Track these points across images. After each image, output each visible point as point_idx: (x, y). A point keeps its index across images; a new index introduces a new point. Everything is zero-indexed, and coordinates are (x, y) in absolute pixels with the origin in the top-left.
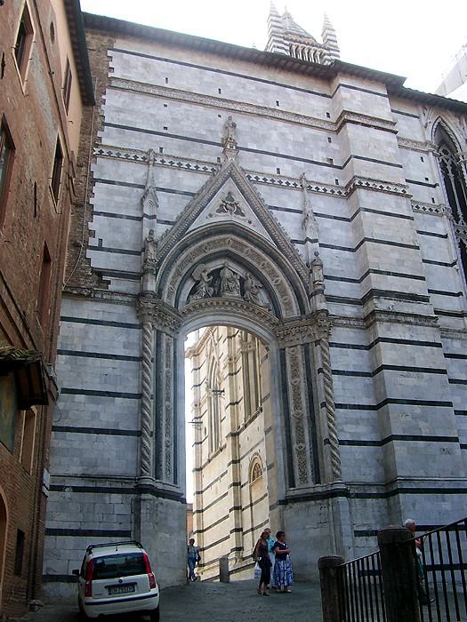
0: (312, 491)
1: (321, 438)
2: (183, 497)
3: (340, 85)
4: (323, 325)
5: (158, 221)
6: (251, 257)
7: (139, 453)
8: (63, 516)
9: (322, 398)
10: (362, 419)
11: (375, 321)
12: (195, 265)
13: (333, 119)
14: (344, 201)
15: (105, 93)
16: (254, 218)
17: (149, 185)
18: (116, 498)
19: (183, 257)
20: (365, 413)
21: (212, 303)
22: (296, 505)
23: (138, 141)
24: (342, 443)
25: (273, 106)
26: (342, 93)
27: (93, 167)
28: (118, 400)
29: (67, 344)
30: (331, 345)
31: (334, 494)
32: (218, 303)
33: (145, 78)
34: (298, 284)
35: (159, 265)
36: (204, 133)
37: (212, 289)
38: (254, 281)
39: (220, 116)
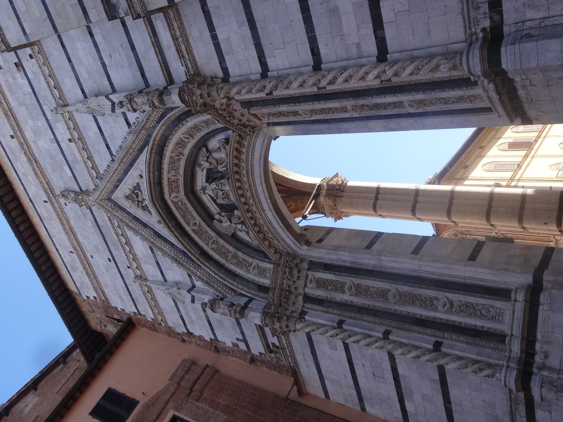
6: (177, 170)
28: (401, 370)
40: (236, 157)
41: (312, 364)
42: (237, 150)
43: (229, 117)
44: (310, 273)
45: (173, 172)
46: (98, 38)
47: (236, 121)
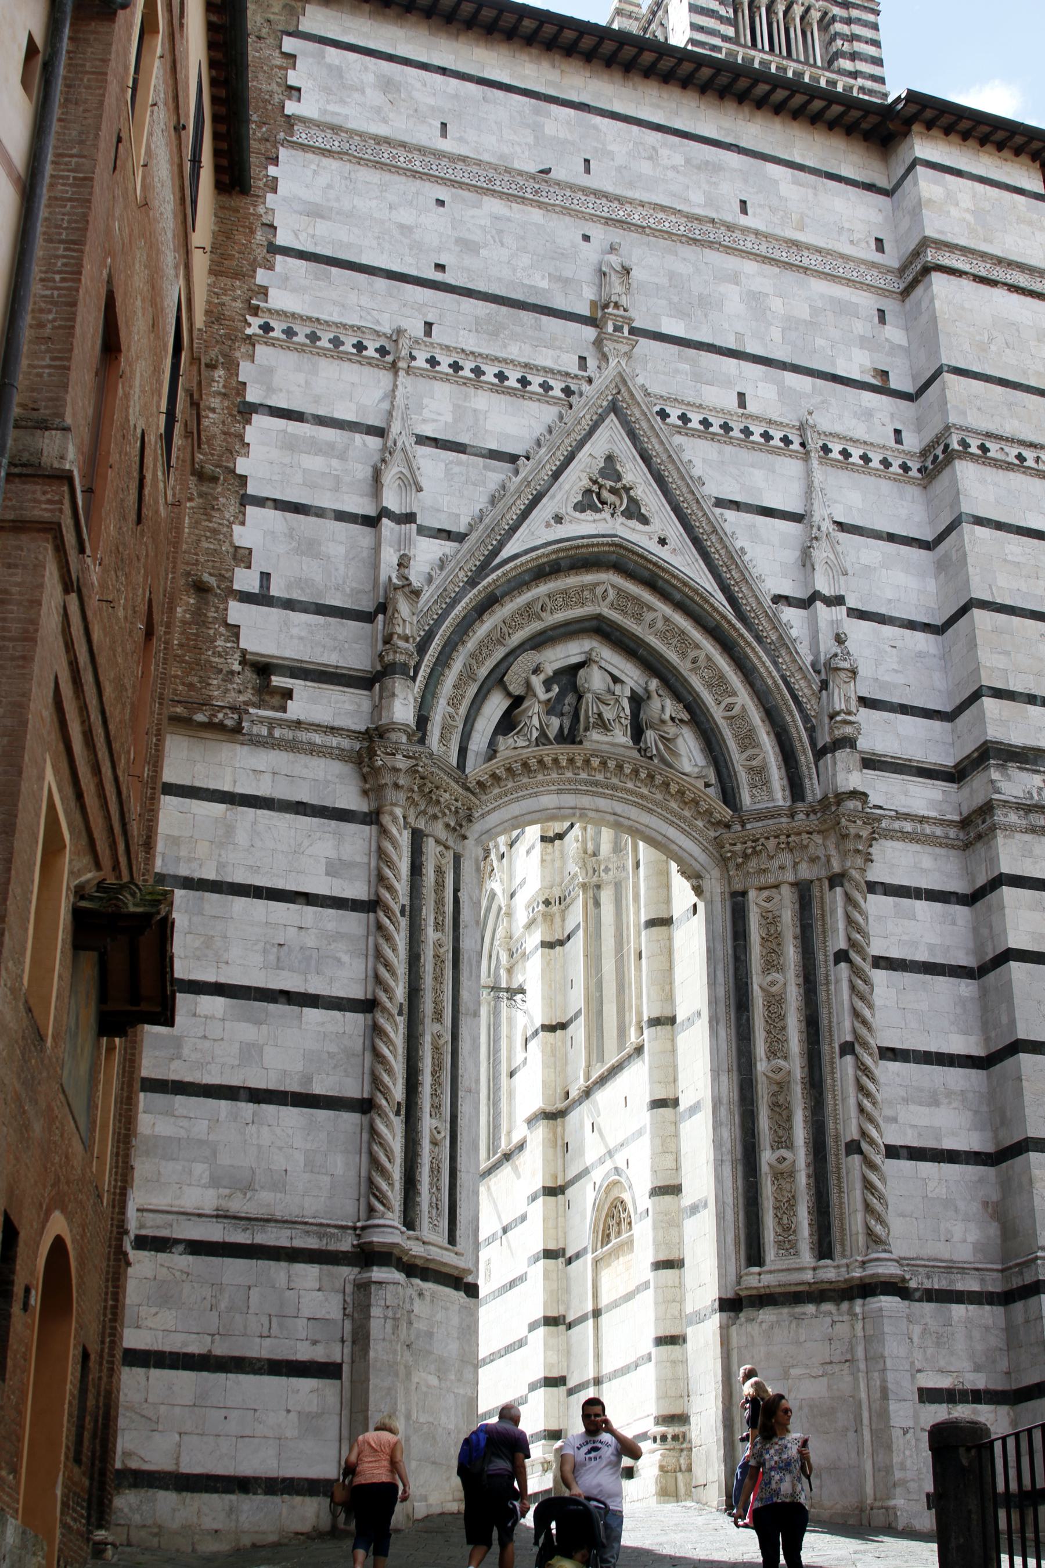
0: (808, 1276)
1: (837, 1137)
2: (470, 1279)
3: (916, 162)
4: (853, 831)
5: (422, 531)
6: (663, 636)
7: (365, 1158)
8: (168, 1318)
9: (844, 1030)
10: (949, 1094)
11: (993, 828)
12: (513, 654)
13: (892, 258)
14: (913, 492)
15: (275, 161)
16: (674, 530)
17: (395, 428)
18: (309, 1273)
19: (482, 629)
20: (956, 1077)
21: (556, 761)
22: (767, 1315)
23: (365, 301)
24: (892, 1152)
25: (731, 213)
26: (923, 184)
27: (246, 371)
28: (311, 1014)
29: (178, 859)
30: (872, 887)
31: (867, 1289)
32: (571, 761)
33: (385, 121)
34: (788, 719)
35: (422, 648)
36: (544, 284)
37: (555, 722)
38: (668, 703)
39: (586, 238)
40: (681, 793)
41: (263, 788)
42: (696, 802)
43: (788, 843)
44: (450, 856)
45: (660, 624)
46: (921, 640)
47: (771, 844)
